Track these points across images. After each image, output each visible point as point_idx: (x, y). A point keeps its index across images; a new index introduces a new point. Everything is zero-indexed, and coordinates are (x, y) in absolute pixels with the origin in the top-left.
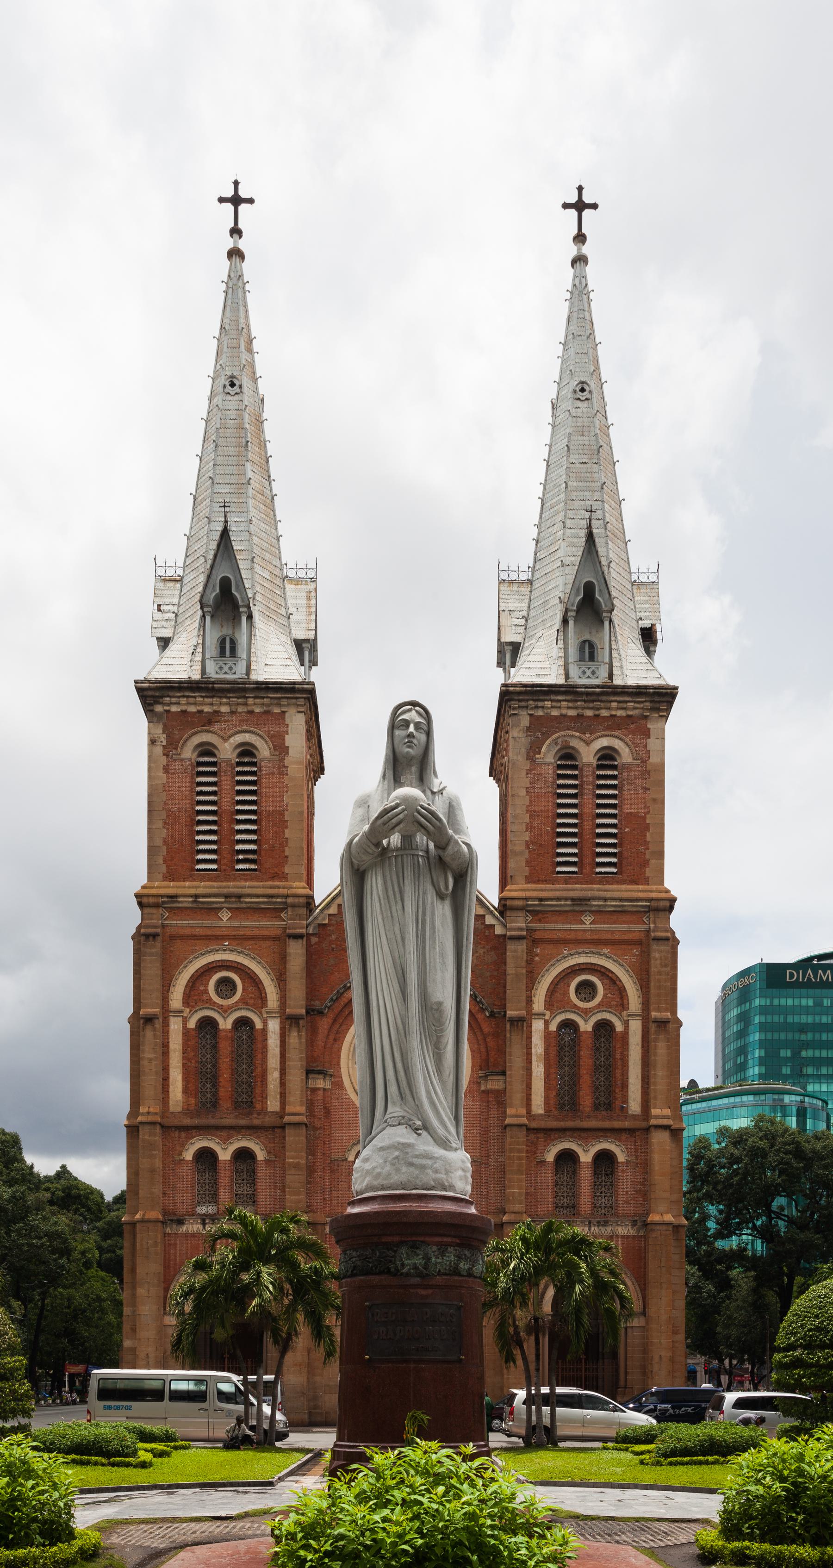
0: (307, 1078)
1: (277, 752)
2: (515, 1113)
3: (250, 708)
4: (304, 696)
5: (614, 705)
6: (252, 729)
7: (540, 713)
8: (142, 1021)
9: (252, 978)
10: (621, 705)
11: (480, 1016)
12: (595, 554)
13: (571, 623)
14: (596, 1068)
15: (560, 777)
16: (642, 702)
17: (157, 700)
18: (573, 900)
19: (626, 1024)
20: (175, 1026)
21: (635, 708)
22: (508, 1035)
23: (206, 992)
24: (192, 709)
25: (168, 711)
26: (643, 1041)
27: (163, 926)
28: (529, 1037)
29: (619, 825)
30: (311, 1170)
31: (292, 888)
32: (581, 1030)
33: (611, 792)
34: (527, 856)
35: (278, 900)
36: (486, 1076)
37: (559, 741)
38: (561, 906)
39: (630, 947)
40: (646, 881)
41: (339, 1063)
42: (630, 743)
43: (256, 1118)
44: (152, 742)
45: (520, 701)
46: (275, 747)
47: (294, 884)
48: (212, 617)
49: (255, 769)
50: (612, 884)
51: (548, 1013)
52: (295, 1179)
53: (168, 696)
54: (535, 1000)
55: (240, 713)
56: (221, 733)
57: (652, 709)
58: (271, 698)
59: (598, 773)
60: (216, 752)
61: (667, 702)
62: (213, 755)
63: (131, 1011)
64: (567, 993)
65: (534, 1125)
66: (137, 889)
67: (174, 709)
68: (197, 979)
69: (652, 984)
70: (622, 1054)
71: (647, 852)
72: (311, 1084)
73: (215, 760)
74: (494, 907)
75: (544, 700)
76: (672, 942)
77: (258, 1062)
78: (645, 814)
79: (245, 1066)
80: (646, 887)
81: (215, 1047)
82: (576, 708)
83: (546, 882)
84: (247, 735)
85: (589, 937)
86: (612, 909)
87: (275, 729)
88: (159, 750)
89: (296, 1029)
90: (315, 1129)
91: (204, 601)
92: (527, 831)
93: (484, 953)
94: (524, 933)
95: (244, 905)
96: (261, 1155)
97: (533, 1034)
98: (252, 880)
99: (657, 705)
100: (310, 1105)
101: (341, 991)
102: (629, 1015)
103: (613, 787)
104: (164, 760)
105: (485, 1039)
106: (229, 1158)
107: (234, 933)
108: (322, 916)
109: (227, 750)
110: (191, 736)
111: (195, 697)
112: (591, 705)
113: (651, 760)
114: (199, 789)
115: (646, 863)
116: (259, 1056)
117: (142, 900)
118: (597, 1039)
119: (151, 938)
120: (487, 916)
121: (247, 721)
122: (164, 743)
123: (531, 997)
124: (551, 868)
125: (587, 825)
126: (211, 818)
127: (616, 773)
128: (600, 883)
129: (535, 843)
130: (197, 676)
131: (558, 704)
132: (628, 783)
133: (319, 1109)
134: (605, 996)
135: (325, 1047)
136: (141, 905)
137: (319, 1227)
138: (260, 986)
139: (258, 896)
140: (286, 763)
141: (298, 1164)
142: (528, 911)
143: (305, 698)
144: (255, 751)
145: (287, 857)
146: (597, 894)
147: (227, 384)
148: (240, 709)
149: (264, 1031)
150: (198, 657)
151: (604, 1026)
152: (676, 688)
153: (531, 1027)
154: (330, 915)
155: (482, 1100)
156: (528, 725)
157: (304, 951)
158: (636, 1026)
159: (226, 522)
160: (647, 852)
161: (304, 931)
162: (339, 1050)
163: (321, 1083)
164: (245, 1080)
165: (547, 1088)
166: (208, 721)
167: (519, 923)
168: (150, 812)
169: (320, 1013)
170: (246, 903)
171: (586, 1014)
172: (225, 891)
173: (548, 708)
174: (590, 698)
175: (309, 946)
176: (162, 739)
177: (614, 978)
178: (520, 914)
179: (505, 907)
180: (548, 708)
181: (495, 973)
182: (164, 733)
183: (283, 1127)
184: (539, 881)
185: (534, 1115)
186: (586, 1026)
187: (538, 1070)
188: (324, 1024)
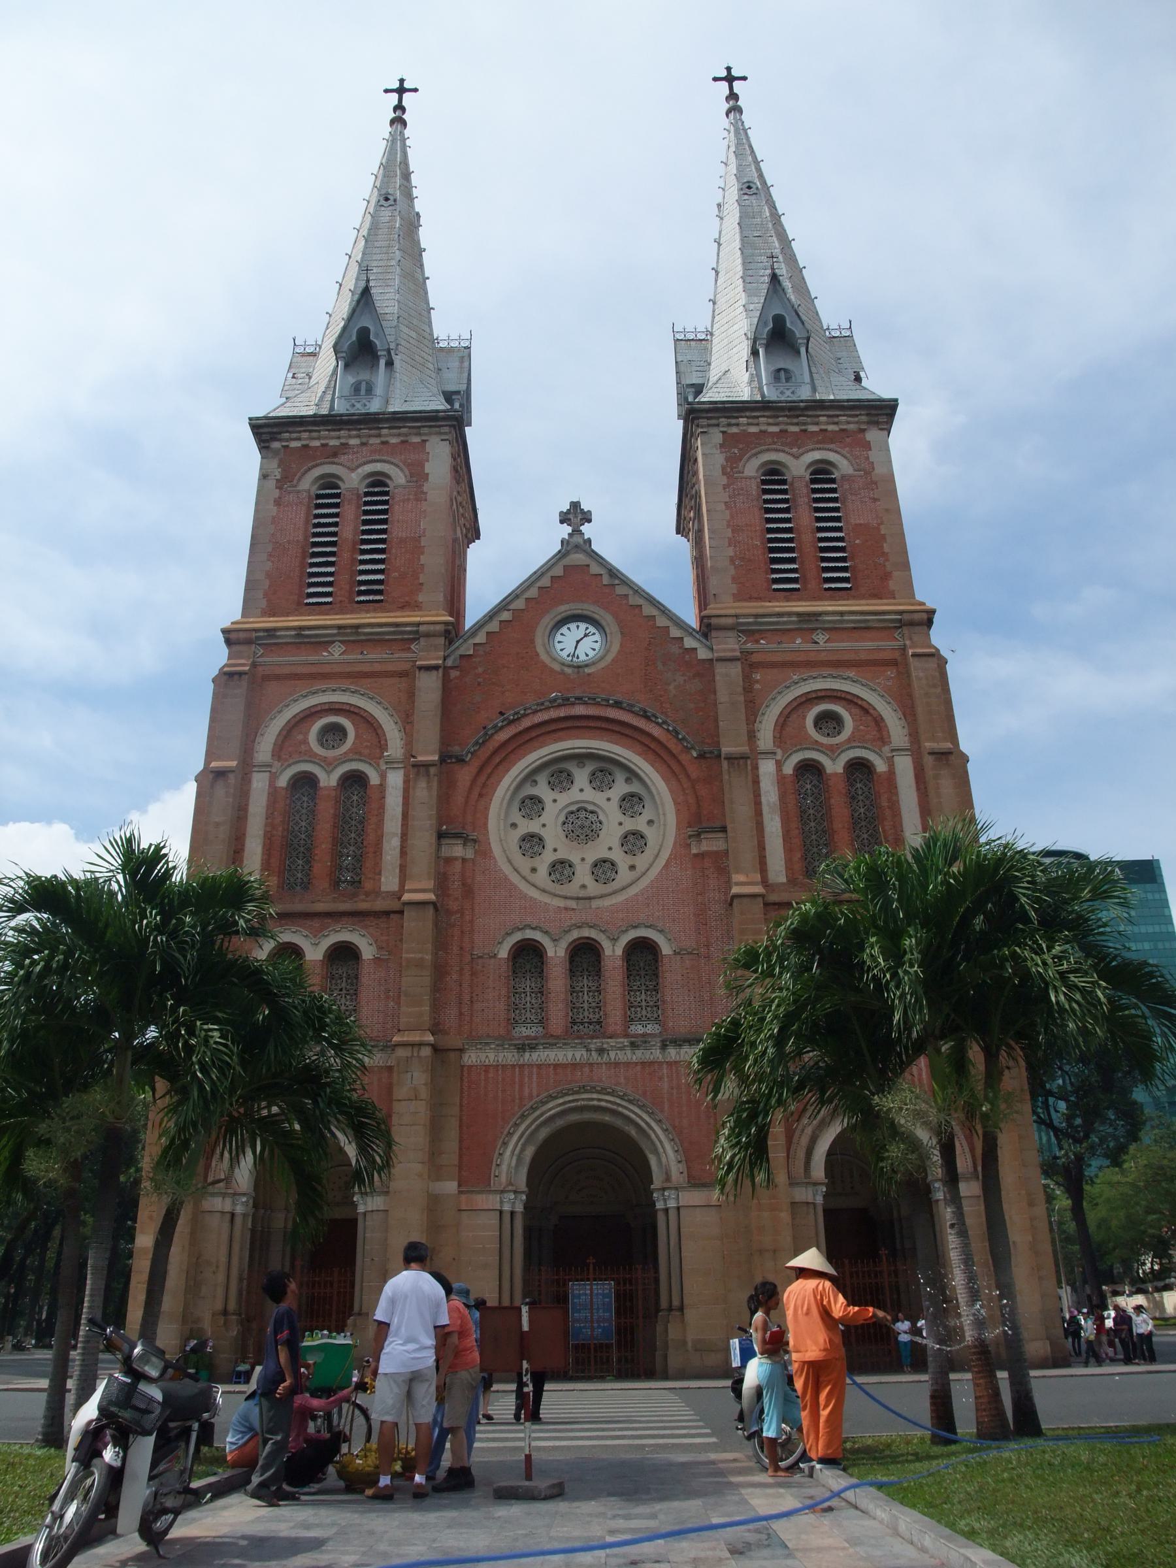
0: (439, 845)
1: (415, 479)
2: (744, 883)
3: (383, 439)
4: (449, 423)
7: (734, 430)
8: (211, 776)
9: (368, 721)
10: (831, 420)
11: (684, 758)
12: (781, 292)
13: (761, 351)
14: (855, 822)
15: (765, 492)
16: (857, 416)
18: (798, 614)
19: (890, 762)
20: (259, 783)
21: (849, 423)
22: (726, 777)
23: (305, 742)
24: (317, 443)
25: (287, 446)
26: (917, 783)
27: (254, 665)
28: (756, 782)
29: (846, 538)
30: (440, 971)
32: (828, 771)
33: (831, 505)
34: (732, 571)
35: (408, 629)
36: (699, 835)
38: (785, 623)
39: (883, 668)
40: (892, 596)
41: (486, 824)
42: (848, 455)
43: (363, 901)
44: (264, 476)
45: (708, 418)
46: (411, 473)
48: (347, 366)
49: (387, 498)
51: (779, 751)
52: (417, 982)
55: (372, 445)
56: (348, 464)
57: (868, 423)
58: (410, 427)
59: (813, 486)
60: (340, 483)
61: (887, 415)
62: (338, 487)
63: (201, 767)
65: (773, 898)
66: (227, 624)
67: (294, 444)
68: (293, 727)
69: (920, 710)
70: (889, 800)
71: (887, 563)
72: (446, 851)
73: (339, 491)
74: (694, 630)
75: (737, 418)
76: (938, 661)
78: (879, 524)
79: (353, 835)
80: (892, 601)
81: (312, 812)
83: (759, 599)
85: (826, 659)
86: (853, 625)
88: (271, 484)
90: (449, 913)
91: (338, 348)
92: (730, 545)
94: (738, 654)
95: (363, 638)
96: (367, 951)
97: (761, 778)
98: (375, 610)
99: (876, 419)
100: (442, 883)
101: (489, 733)
102: (893, 750)
103: (835, 500)
104: (277, 493)
105: (693, 787)
106: (321, 958)
107: (347, 670)
108: (465, 646)
109: (353, 480)
110: (309, 469)
111: (319, 431)
112: (795, 421)
113: (876, 471)
114: (316, 521)
115: (886, 576)
117: (231, 637)
118: (852, 785)
119: (236, 677)
120: (685, 639)
122: (278, 477)
123: (754, 732)
124: (765, 584)
125: (807, 538)
126: (328, 549)
127: (834, 486)
128: (832, 598)
129: (742, 559)
130: (325, 412)
131: (755, 421)
132: (851, 494)
133: (455, 886)
134: (856, 728)
135: (466, 802)
136: (228, 642)
137: (452, 1055)
138: (379, 731)
142: (739, 631)
144: (388, 481)
145: (422, 584)
146: (830, 609)
147: (382, 199)
148: (372, 441)
149: (382, 787)
150: (329, 397)
151: (859, 767)
152: (896, 400)
153: (756, 768)
154: (475, 644)
157: (440, 686)
158: (904, 766)
159: (368, 281)
160: (887, 563)
162: (487, 809)
163: (457, 850)
165: (788, 849)
166: (333, 454)
167: (729, 644)
168: (252, 545)
169: (461, 760)
171: (832, 751)
174: (792, 413)
175: (446, 680)
176: (277, 473)
177: (864, 704)
178: (730, 634)
179: (707, 628)
180: (744, 425)
182: (279, 466)
183: (401, 912)
185: (772, 885)
186: (834, 767)
187: (773, 826)
188: (464, 775)
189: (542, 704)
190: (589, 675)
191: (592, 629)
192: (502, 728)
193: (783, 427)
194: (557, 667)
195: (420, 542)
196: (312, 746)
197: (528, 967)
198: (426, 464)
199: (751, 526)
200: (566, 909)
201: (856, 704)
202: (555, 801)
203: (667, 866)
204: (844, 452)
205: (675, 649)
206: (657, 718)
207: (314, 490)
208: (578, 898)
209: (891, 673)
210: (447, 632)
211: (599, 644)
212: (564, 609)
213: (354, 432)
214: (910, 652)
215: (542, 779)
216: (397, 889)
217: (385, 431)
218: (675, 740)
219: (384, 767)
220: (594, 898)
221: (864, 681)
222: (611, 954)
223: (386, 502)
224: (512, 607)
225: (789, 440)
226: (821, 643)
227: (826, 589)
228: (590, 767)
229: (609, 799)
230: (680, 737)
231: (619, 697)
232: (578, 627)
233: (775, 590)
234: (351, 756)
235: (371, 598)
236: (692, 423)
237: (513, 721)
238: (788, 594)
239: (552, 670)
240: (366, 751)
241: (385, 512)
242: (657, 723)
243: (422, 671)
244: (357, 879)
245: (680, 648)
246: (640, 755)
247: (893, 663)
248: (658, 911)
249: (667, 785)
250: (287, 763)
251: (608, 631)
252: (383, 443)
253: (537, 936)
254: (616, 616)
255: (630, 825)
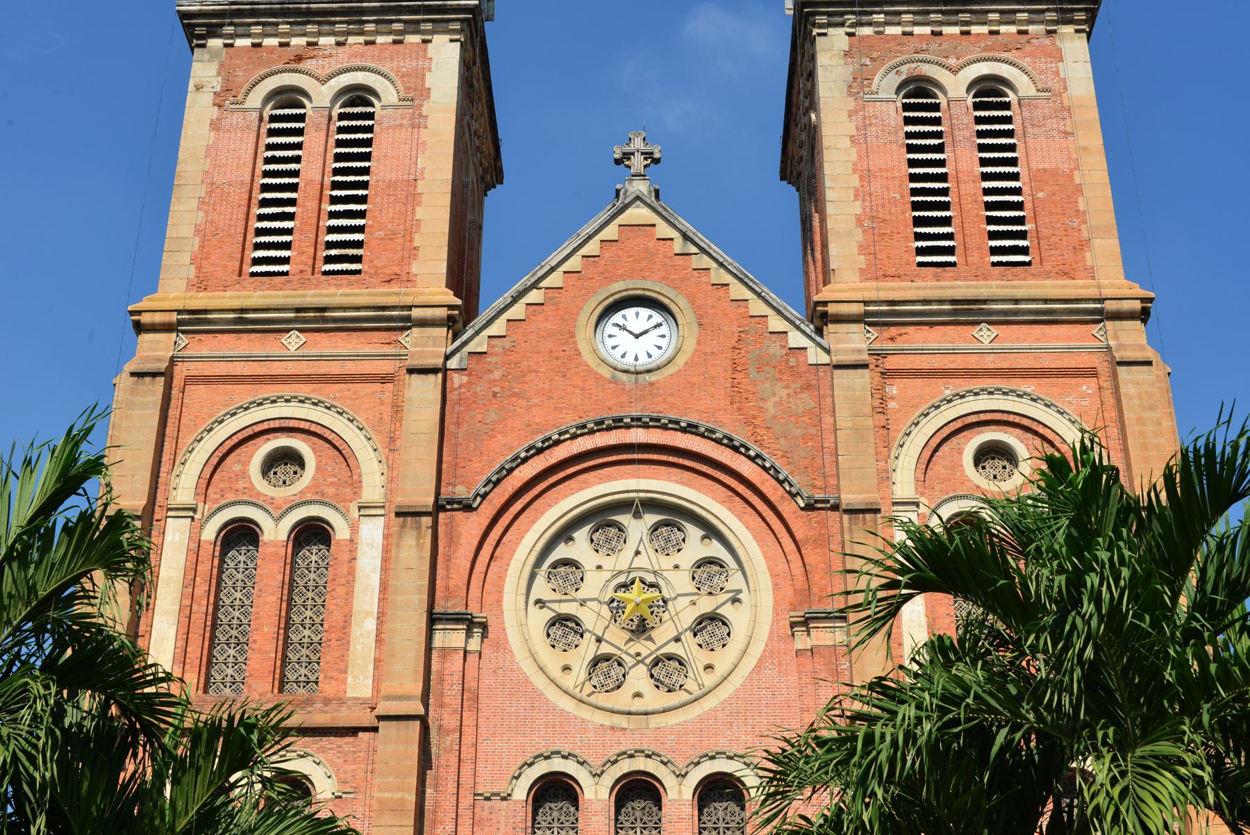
5: (994, 16)
6: (370, 64)
11: (787, 508)
17: (213, 31)
23: (244, 475)
25: (231, 45)
27: (173, 361)
29: (1026, 190)
31: (422, 294)
34: (859, 236)
36: (806, 622)
37: (904, 68)
38: (931, 313)
39: (1074, 381)
41: (499, 602)
46: (407, 89)
47: (427, 291)
49: (371, 123)
50: (1025, 279)
53: (231, 24)
54: (896, 477)
55: (351, 45)
56: (319, 72)
64: (957, 466)
71: (1083, 227)
73: (302, 111)
77: (333, 603)
79: (309, 613)
82: (927, 24)
84: (360, 74)
87: (409, 65)
89: (414, 533)
92: (856, 199)
93: (788, 395)
94: (865, 357)
98: (350, 284)
108: (477, 339)
109: (321, 96)
112: (953, 18)
114: (269, 154)
116: (341, 590)
121: (362, 56)
127: (1008, 113)
128: (1002, 277)
131: (896, 19)
132: (1033, 125)
133: (450, 692)
139: (358, 309)
140: (425, 111)
141: (402, 800)
143: (461, 20)
154: (489, 337)
155: (799, 672)
156: (847, 49)
160: (1083, 227)
161: (439, 362)
162: (502, 577)
164: (306, 640)
169: (467, 508)
170: (335, 320)
172: (298, 302)
173: (878, 24)
180: (878, 24)
181: (813, 431)
182: (219, 74)
184: (885, 276)
188: (470, 526)
189: (584, 426)
190: (651, 384)
191: (657, 318)
192: (525, 460)
193: (937, 29)
194: (606, 372)
195: (415, 187)
196: (254, 481)
197: (555, 814)
198: (428, 74)
199: (886, 170)
200: (612, 728)
201: (1036, 433)
202: (599, 567)
203: (758, 667)
204: (1025, 62)
205: (775, 349)
206: (748, 449)
207: (268, 112)
208: (629, 713)
209: (1087, 386)
210: (450, 322)
211: (666, 339)
212: (619, 287)
213: (326, 28)
214: (1116, 355)
215: (582, 535)
216: (370, 695)
217: (370, 27)
218: (774, 482)
219: (354, 513)
220: (653, 713)
221: (1048, 399)
222: (676, 797)
223: (369, 129)
224: (542, 284)
225: (945, 46)
226: (986, 343)
227: (994, 264)
228: (651, 519)
229: (676, 567)
230: (781, 477)
231: (694, 419)
232: (637, 314)
233: (920, 264)
234: (309, 497)
235: (345, 266)
236: (807, 20)
237: (540, 451)
238: (939, 270)
239: (599, 378)
240: (331, 491)
241: (368, 143)
242: (749, 457)
243: (414, 376)
244: (313, 678)
245: (783, 347)
246: (722, 503)
247: (1091, 373)
248: (746, 734)
249: (761, 547)
250: (216, 506)
251: (680, 322)
252: (367, 43)
253: (569, 767)
254: (692, 301)
255: (706, 605)
